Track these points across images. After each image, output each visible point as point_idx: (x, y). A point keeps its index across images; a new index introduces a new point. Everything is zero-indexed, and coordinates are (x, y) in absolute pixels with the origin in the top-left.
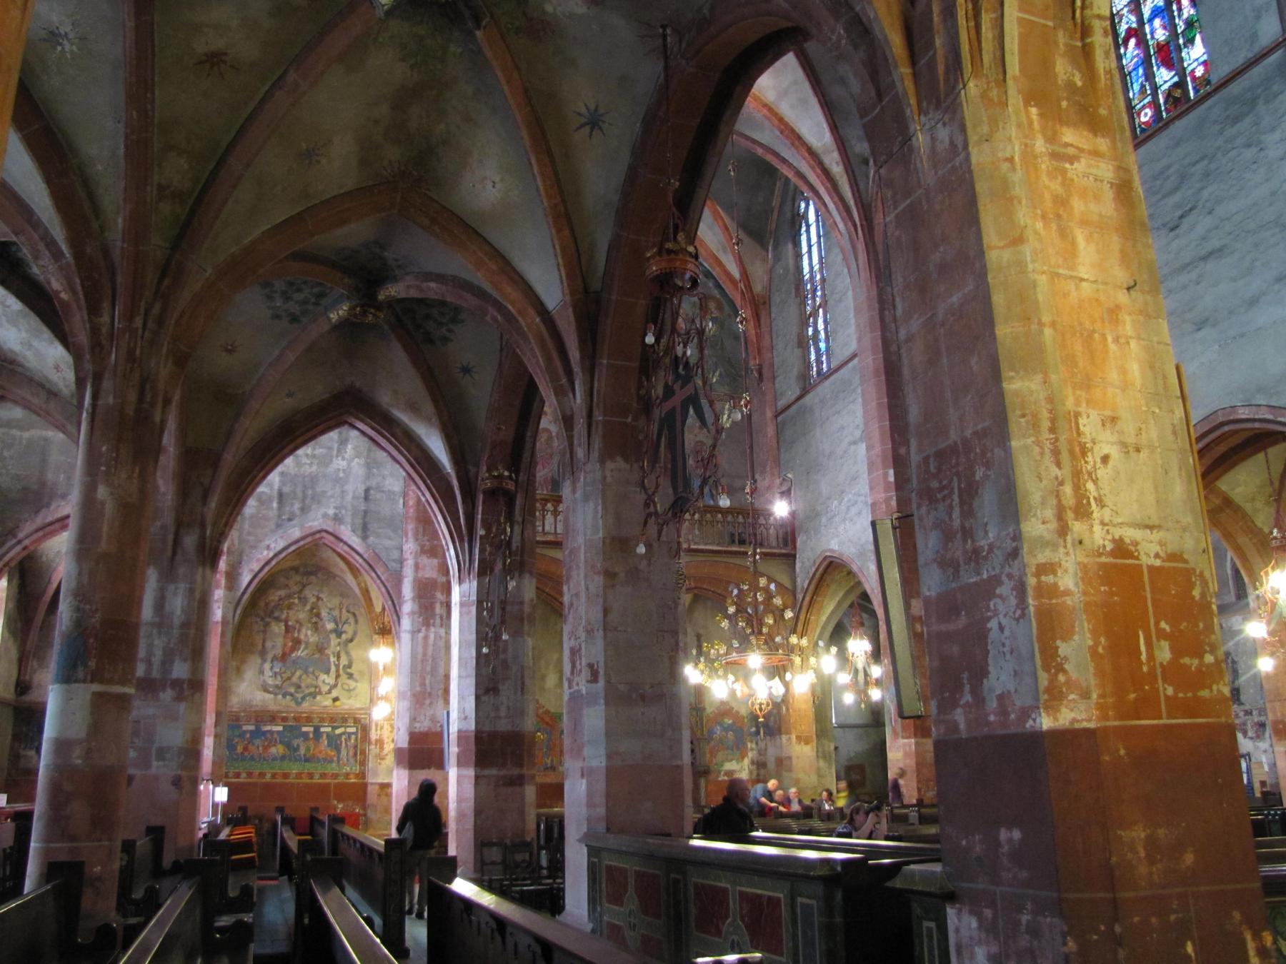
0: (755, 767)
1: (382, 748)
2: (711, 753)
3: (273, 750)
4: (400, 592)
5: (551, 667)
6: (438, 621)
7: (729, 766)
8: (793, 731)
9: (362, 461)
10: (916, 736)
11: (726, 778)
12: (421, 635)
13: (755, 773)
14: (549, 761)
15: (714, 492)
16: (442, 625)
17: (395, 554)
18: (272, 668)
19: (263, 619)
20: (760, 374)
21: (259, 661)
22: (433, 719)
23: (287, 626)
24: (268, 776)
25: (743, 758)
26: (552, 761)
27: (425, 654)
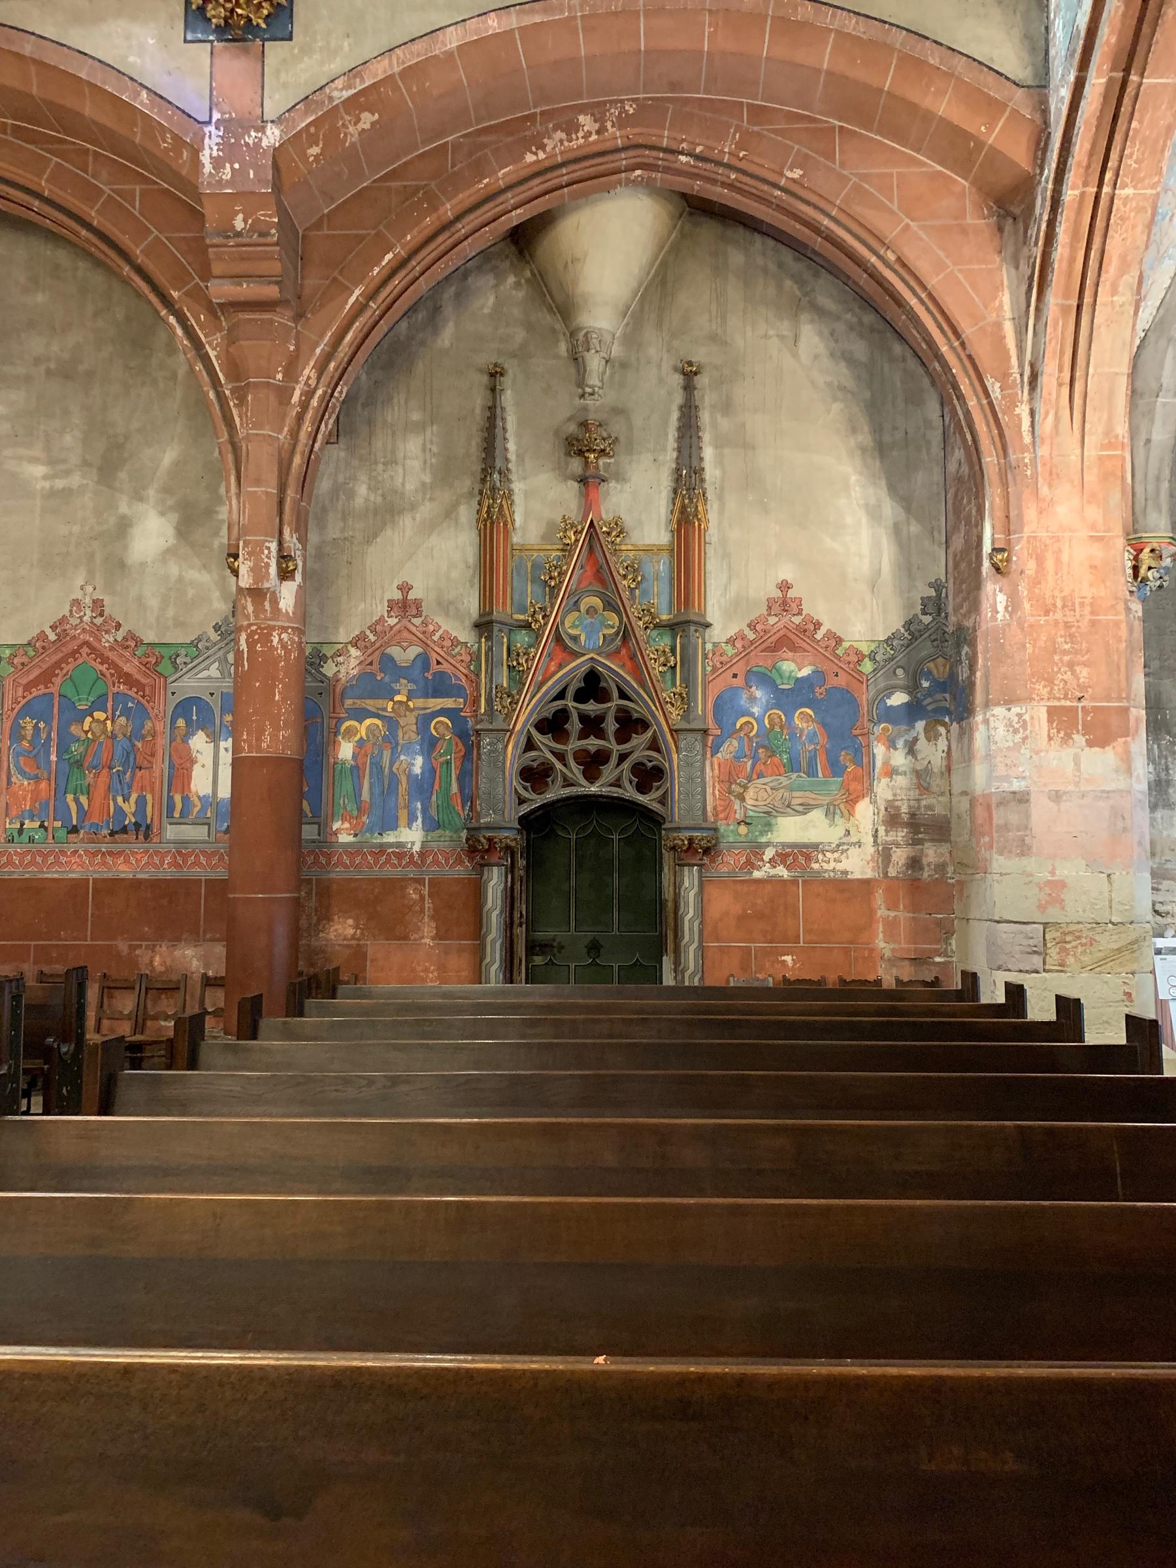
0: (900, 835)
2: (729, 778)
5: (151, 493)
11: (782, 872)
13: (900, 856)
14: (129, 808)
25: (852, 802)
26: (141, 802)
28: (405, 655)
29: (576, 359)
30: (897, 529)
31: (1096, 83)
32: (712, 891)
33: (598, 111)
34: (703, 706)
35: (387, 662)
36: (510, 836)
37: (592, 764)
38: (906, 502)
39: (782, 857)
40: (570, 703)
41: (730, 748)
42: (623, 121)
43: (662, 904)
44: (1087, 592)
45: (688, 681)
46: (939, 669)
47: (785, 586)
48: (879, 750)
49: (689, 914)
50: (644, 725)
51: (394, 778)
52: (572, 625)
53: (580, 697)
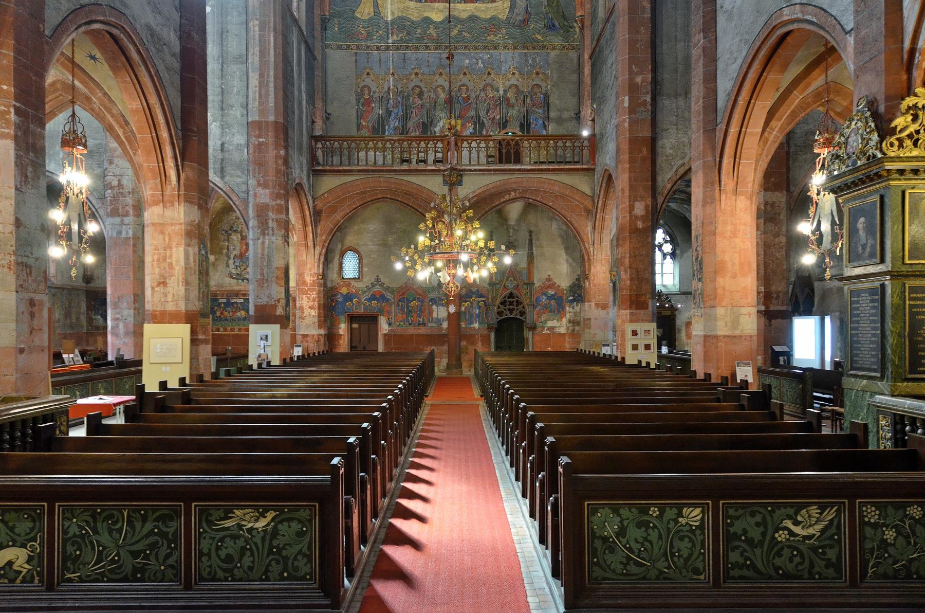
0: (571, 324)
1: (303, 312)
2: (538, 314)
3: (239, 314)
4: (247, 213)
6: (271, 232)
7: (550, 324)
8: (594, 300)
9: (218, 124)
10: (630, 308)
11: (548, 332)
12: (260, 242)
13: (571, 328)
14: (421, 320)
15: (547, 123)
16: (273, 235)
17: (244, 188)
18: (234, 263)
19: (226, 232)
20: (582, 22)
21: (226, 258)
22: (270, 296)
23: (241, 235)
24: (236, 330)
25: (562, 318)
26: (423, 319)
27: (263, 254)
28: (474, 290)
29: (507, 229)
30: (571, 265)
31: (600, 202)
32: (535, 336)
33: (515, 191)
34: (534, 299)
35: (471, 290)
36: (496, 326)
37: (511, 311)
38: (573, 259)
39: (548, 329)
40: (507, 299)
41: (539, 308)
42: (520, 193)
43: (524, 339)
44: (602, 282)
45: (531, 295)
46: (579, 292)
47: (549, 276)
48: (567, 308)
49: (530, 340)
50: (521, 303)
51: (473, 314)
52: (508, 284)
53: (509, 298)
